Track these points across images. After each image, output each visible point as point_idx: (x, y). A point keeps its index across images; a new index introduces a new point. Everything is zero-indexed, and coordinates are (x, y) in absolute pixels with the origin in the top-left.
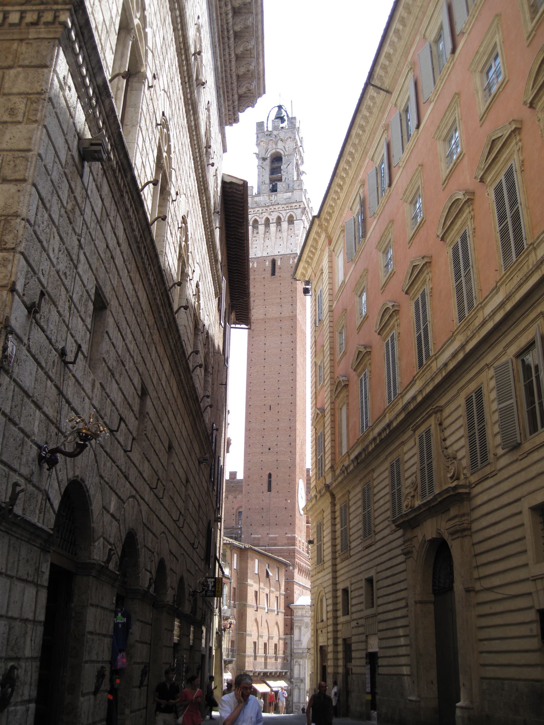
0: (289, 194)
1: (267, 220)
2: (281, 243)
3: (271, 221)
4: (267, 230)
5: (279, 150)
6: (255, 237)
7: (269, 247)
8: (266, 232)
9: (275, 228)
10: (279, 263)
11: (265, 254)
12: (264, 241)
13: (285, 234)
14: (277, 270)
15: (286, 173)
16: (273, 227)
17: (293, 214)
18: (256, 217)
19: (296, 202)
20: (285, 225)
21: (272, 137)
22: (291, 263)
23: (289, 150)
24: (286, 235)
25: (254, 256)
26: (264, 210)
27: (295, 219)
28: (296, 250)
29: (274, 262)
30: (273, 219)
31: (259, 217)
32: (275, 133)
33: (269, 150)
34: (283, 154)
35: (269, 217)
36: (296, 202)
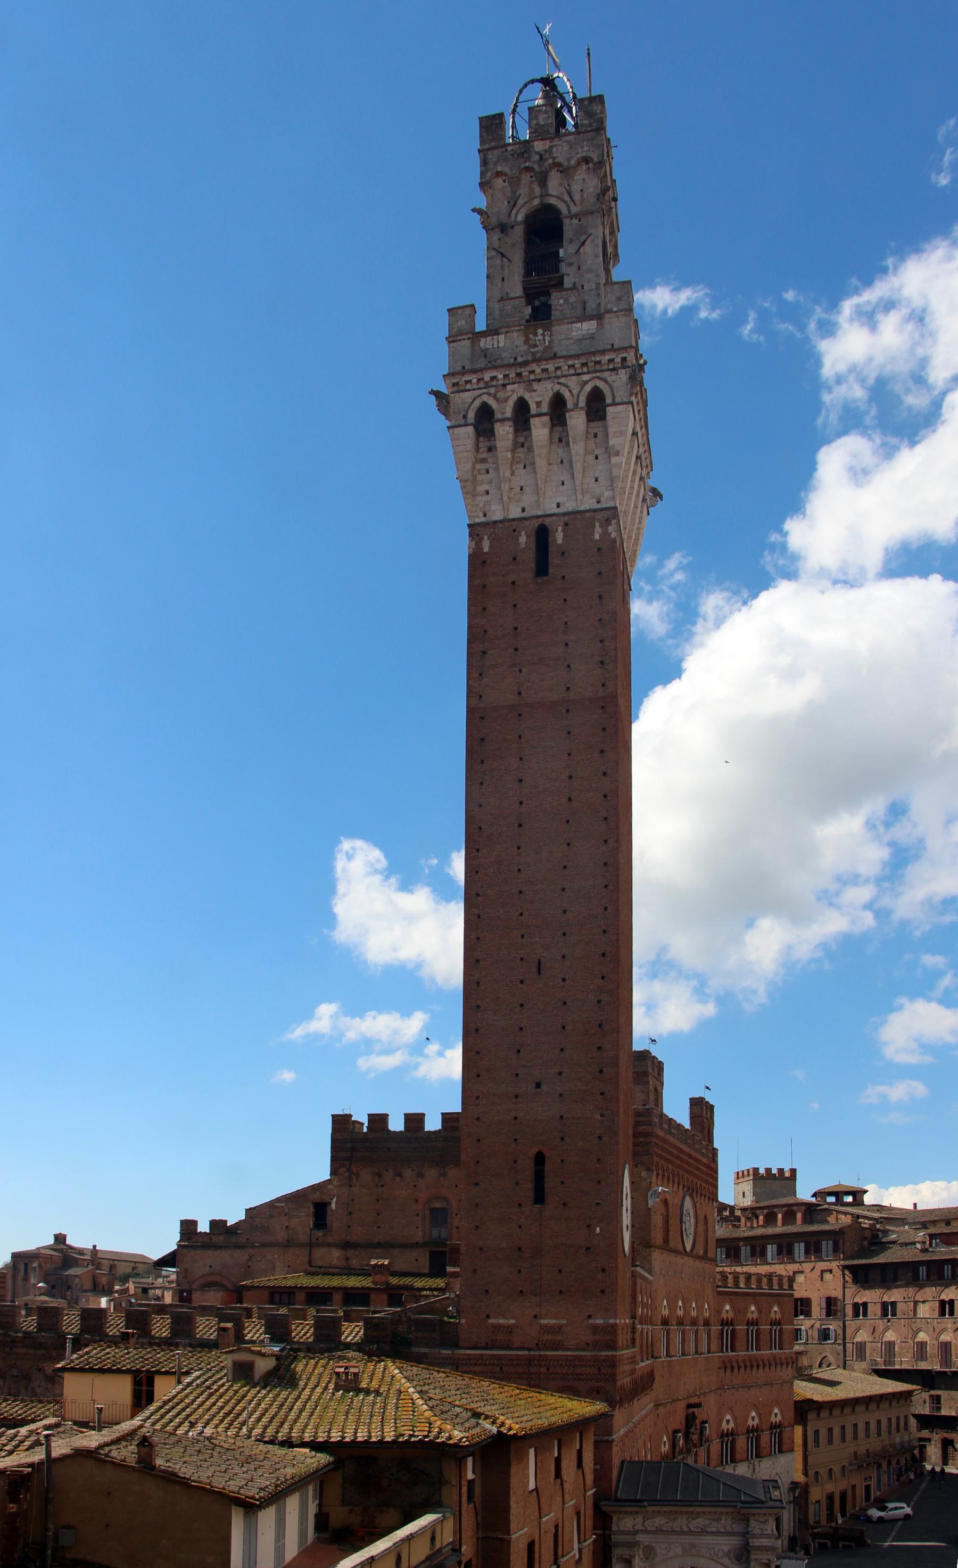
0: (589, 326)
1: (522, 407)
2: (566, 477)
3: (533, 409)
4: (521, 440)
5: (552, 201)
6: (484, 461)
7: (527, 490)
8: (517, 445)
9: (546, 431)
10: (559, 537)
11: (515, 513)
12: (513, 474)
13: (577, 449)
14: (554, 560)
15: (574, 268)
16: (540, 430)
17: (601, 385)
18: (485, 398)
19: (613, 349)
20: (577, 421)
21: (529, 159)
22: (597, 537)
23: (582, 199)
24: (581, 451)
25: (483, 520)
26: (512, 375)
27: (609, 401)
28: (613, 498)
29: (542, 535)
30: (538, 404)
31: (495, 397)
32: (539, 146)
33: (521, 202)
34: (564, 211)
35: (527, 396)
36: (613, 349)
